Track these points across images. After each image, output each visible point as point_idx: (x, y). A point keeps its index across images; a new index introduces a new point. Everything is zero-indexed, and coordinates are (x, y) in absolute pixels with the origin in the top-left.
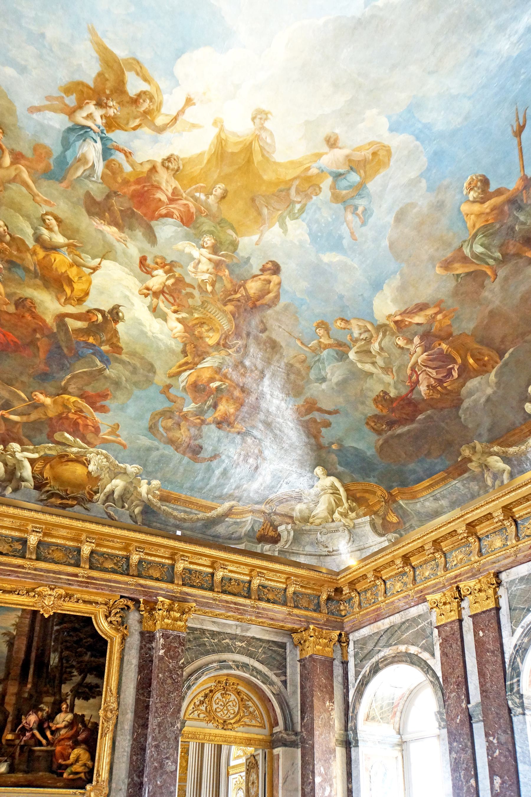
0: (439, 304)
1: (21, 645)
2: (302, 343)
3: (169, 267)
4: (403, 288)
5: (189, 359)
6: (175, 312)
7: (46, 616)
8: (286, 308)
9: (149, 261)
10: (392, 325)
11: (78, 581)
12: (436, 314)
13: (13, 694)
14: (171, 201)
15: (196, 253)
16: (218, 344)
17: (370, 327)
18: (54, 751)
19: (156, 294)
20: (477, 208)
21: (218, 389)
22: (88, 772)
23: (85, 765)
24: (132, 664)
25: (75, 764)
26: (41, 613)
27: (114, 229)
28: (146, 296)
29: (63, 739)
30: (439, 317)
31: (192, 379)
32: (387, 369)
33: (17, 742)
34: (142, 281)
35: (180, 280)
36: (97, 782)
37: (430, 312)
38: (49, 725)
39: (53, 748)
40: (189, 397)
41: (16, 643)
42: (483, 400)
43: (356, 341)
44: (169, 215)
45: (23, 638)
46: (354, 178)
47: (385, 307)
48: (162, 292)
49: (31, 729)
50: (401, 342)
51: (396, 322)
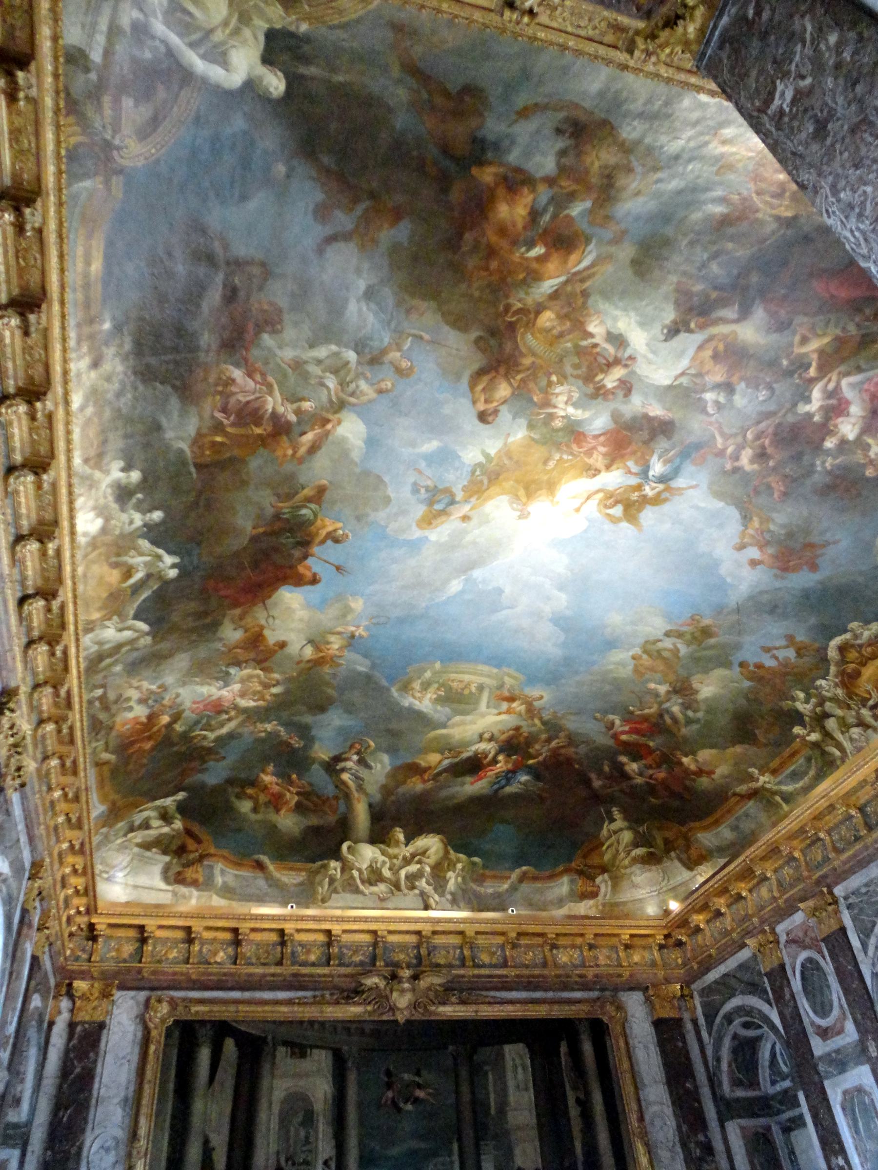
0: (301, 461)
2: (421, 338)
3: (599, 393)
4: (345, 453)
5: (579, 287)
6: (596, 345)
8: (458, 377)
9: (620, 393)
10: (330, 417)
12: (295, 452)
14: (594, 448)
15: (571, 410)
16: (538, 313)
17: (352, 400)
19: (617, 362)
20: (330, 529)
21: (531, 245)
27: (651, 414)
28: (631, 358)
30: (290, 452)
31: (573, 258)
32: (298, 365)
34: (633, 373)
35: (588, 378)
37: (302, 451)
40: (583, 225)
42: (164, 422)
43: (358, 376)
44: (596, 437)
46: (438, 507)
47: (350, 429)
48: (609, 365)
50: (307, 405)
51: (328, 421)
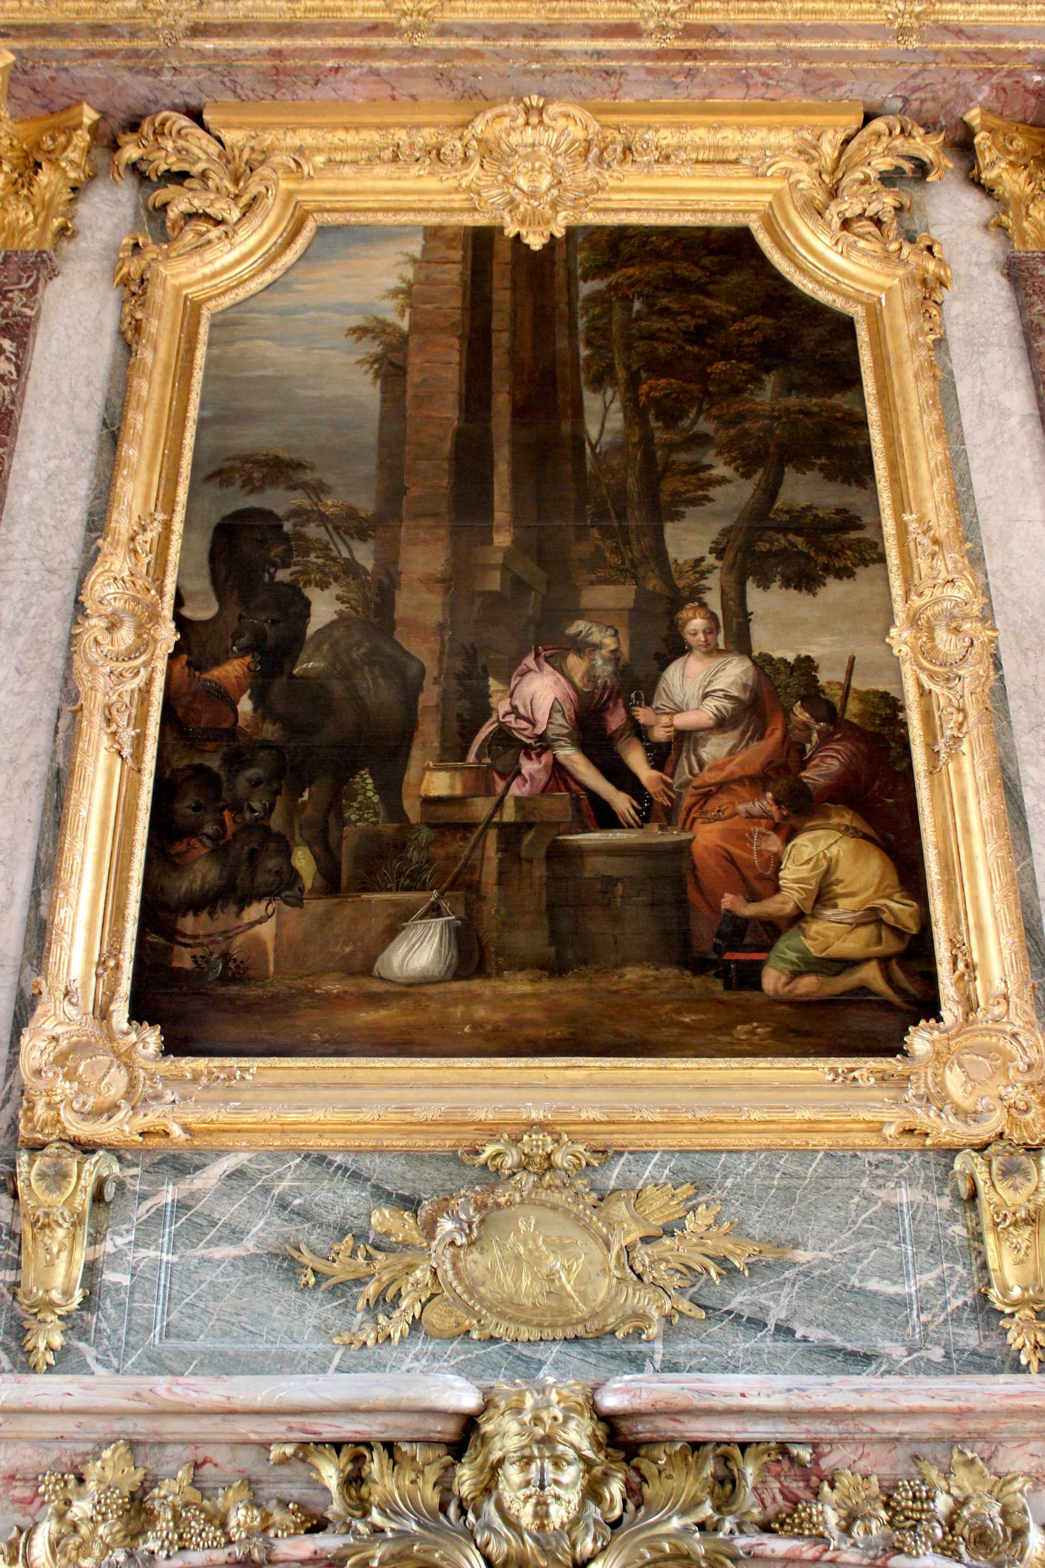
1: (441, 366)
7: (535, 242)
11: (643, 55)
13: (428, 581)
18: (682, 850)
23: (873, 917)
24: (1004, 414)
25: (814, 916)
26: (511, 231)
29: (722, 787)
36: (970, 1006)
39: (674, 836)
41: (415, 361)
45: (443, 338)
49: (544, 744)
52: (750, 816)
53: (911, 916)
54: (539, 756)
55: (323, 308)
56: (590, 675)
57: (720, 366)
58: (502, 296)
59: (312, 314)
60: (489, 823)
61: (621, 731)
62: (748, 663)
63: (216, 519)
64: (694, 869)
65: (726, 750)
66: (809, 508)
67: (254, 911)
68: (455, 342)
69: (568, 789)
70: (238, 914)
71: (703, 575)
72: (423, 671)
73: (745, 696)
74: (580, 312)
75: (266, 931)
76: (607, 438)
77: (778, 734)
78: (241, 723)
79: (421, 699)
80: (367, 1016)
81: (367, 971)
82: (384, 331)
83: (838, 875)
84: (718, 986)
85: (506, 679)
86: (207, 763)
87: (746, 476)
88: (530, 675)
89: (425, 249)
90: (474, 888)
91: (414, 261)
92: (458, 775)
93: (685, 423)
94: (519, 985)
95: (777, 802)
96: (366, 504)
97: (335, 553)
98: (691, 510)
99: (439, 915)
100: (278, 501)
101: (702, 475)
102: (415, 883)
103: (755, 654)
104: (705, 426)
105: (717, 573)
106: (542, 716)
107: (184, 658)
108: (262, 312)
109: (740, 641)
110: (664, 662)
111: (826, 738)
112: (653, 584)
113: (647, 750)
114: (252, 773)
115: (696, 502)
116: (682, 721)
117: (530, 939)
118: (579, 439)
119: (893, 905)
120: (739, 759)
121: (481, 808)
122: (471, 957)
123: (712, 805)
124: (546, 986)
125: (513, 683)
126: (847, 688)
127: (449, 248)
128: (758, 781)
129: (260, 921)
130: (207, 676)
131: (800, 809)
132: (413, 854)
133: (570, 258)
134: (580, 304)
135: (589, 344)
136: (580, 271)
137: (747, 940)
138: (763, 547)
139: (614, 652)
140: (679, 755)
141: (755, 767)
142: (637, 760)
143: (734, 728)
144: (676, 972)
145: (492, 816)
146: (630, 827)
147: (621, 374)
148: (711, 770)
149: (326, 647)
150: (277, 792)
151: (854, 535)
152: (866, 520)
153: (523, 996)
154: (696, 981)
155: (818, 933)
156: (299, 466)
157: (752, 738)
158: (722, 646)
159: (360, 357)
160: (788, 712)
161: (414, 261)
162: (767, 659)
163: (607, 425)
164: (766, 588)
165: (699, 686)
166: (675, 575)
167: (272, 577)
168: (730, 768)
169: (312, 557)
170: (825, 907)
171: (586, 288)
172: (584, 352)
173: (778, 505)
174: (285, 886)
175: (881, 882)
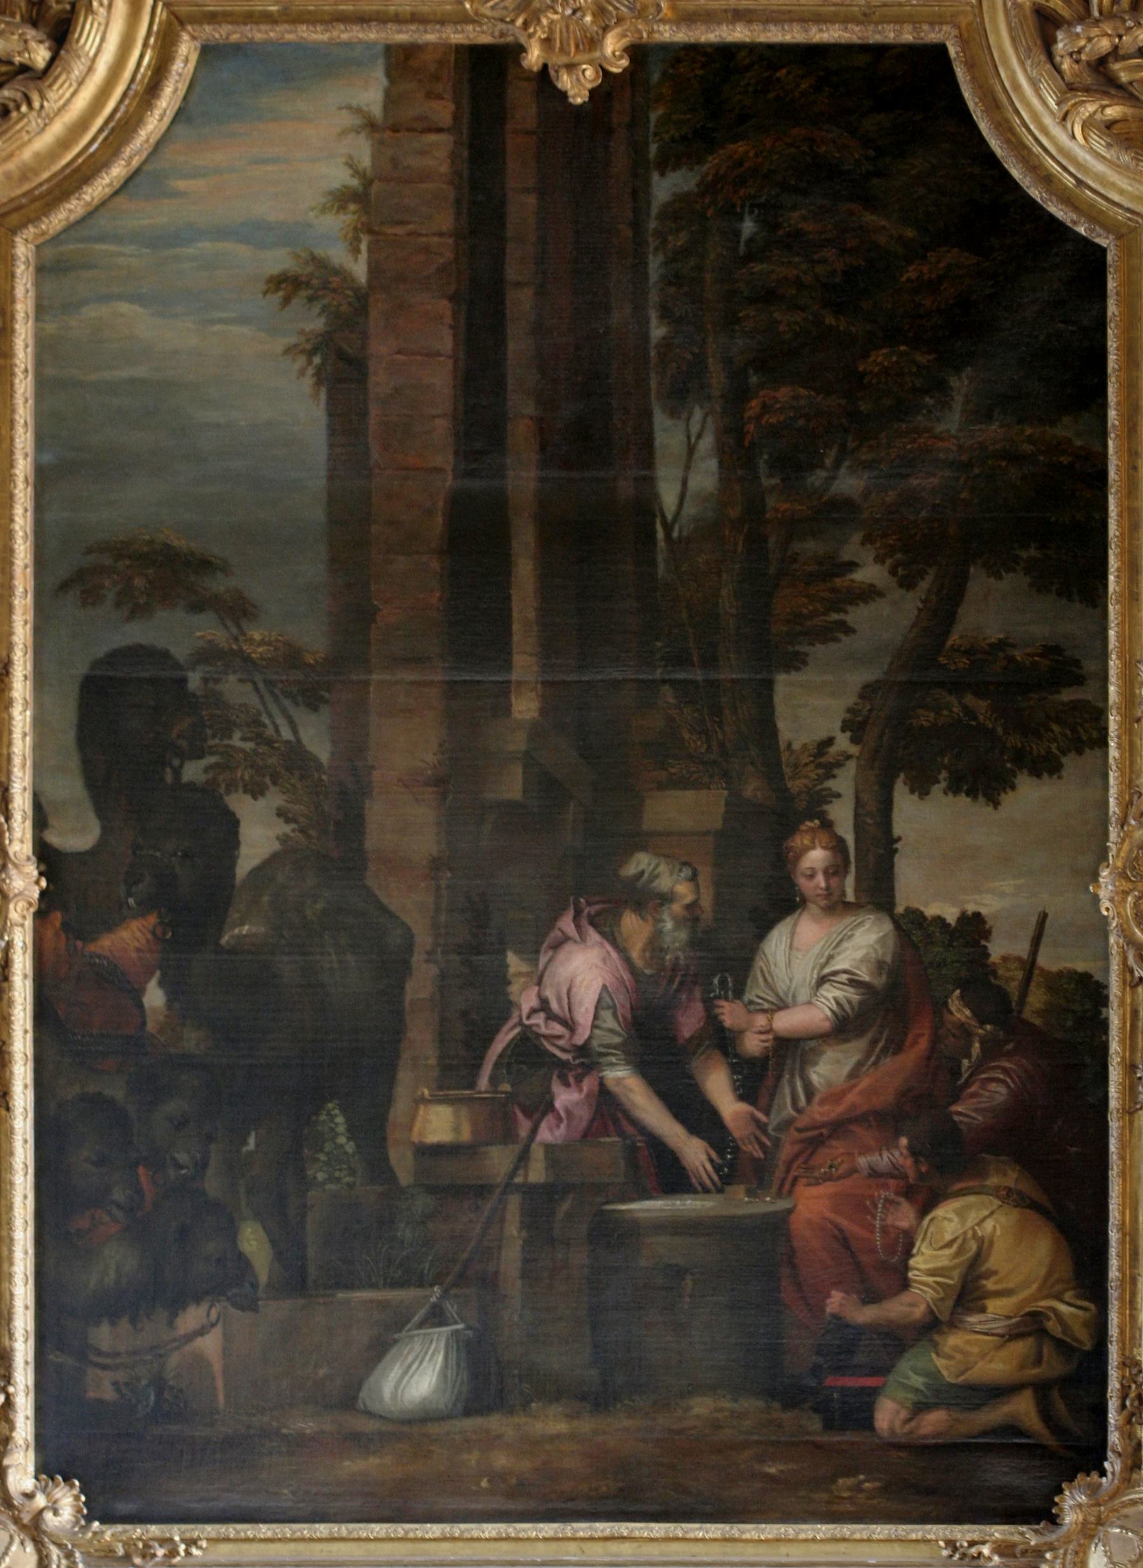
1: (420, 362)
7: (577, 86)
18: (776, 1226)
22: (1065, 1382)
25: (953, 1324)
33: (498, 1160)
38: (712, 1020)
39: (767, 1204)
41: (381, 347)
49: (587, 1059)
52: (874, 1173)
53: (1085, 1324)
54: (579, 1080)
55: (221, 233)
56: (655, 945)
57: (881, 357)
58: (522, 208)
59: (206, 246)
60: (509, 1187)
61: (697, 1040)
62: (888, 926)
63: (81, 669)
64: (791, 1258)
65: (846, 1069)
66: (1002, 645)
67: (192, 1317)
68: (444, 307)
69: (621, 1133)
70: (171, 1324)
71: (829, 770)
72: (409, 946)
73: (880, 982)
74: (653, 243)
75: (210, 1345)
76: (690, 510)
77: (923, 1044)
78: (151, 1026)
79: (409, 986)
80: (353, 1466)
81: (348, 1400)
82: (325, 285)
83: (992, 1263)
84: (815, 1424)
85: (531, 953)
86: (107, 1092)
87: (908, 584)
88: (568, 947)
89: (390, 100)
90: (490, 1282)
91: (371, 126)
92: (464, 1111)
93: (817, 478)
94: (552, 1422)
95: (914, 1152)
96: (313, 638)
97: (270, 732)
98: (819, 651)
99: (442, 1323)
100: (177, 632)
101: (838, 581)
102: (408, 1276)
103: (900, 909)
104: (849, 483)
105: (851, 767)
106: (584, 1014)
107: (57, 917)
108: (118, 239)
109: (878, 892)
110: (764, 928)
111: (992, 1049)
112: (753, 789)
113: (734, 1068)
114: (173, 1107)
115: (827, 634)
116: (787, 1022)
117: (568, 1358)
118: (645, 508)
119: (1063, 1308)
120: (865, 1083)
121: (498, 1160)
122: (486, 1383)
123: (824, 1156)
124: (586, 1425)
125: (543, 960)
126: (1030, 966)
127: (430, 95)
128: (886, 1121)
129: (201, 1332)
130: (92, 948)
131: (946, 1164)
132: (405, 1232)
133: (636, 121)
134: (653, 225)
135: (665, 313)
136: (653, 148)
137: (860, 1358)
138: (925, 718)
139: (692, 907)
140: (779, 1078)
141: (886, 1098)
142: (718, 1086)
143: (860, 1033)
144: (760, 1404)
145: (513, 1174)
146: (706, 1191)
147: (718, 378)
148: (822, 1102)
149: (266, 899)
150: (210, 1138)
151: (1067, 695)
152: (1089, 666)
153: (556, 1438)
154: (787, 1416)
155: (956, 1349)
156: (205, 565)
157: (884, 1051)
158: (850, 897)
159: (293, 340)
160: (941, 1006)
161: (371, 126)
162: (916, 917)
163: (693, 484)
164: (924, 793)
165: (817, 962)
166: (787, 771)
167: (177, 772)
168: (852, 1098)
169: (236, 741)
170: (971, 1311)
171: (665, 188)
172: (658, 331)
173: (953, 639)
174: (230, 1281)
175: (1049, 1274)
